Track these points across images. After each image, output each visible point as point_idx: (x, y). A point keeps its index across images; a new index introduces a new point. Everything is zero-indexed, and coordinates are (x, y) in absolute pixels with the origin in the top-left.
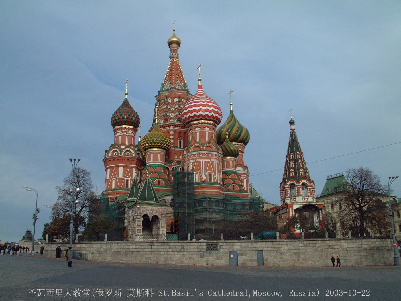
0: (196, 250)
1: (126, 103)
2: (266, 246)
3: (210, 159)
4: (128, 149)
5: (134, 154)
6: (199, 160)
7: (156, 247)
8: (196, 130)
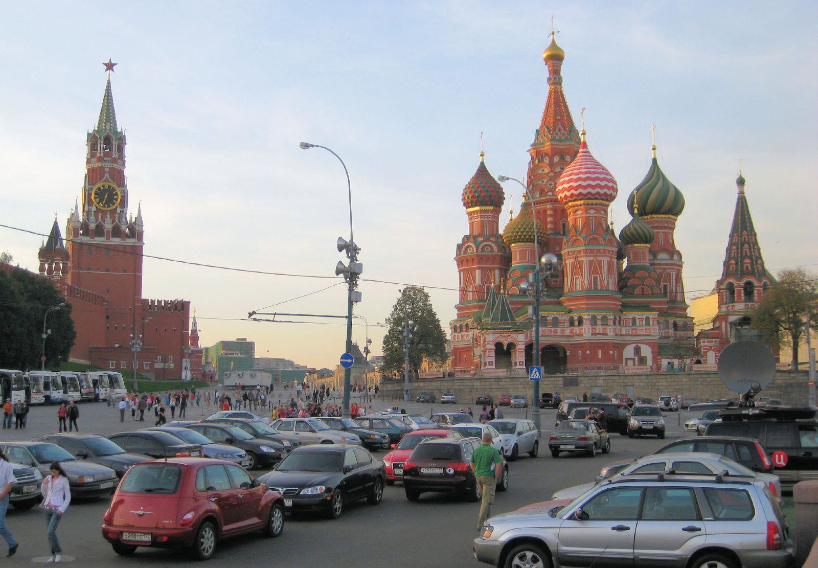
0: (552, 386)
2: (639, 381)
3: (595, 256)
4: (488, 243)
5: (495, 250)
8: (578, 215)
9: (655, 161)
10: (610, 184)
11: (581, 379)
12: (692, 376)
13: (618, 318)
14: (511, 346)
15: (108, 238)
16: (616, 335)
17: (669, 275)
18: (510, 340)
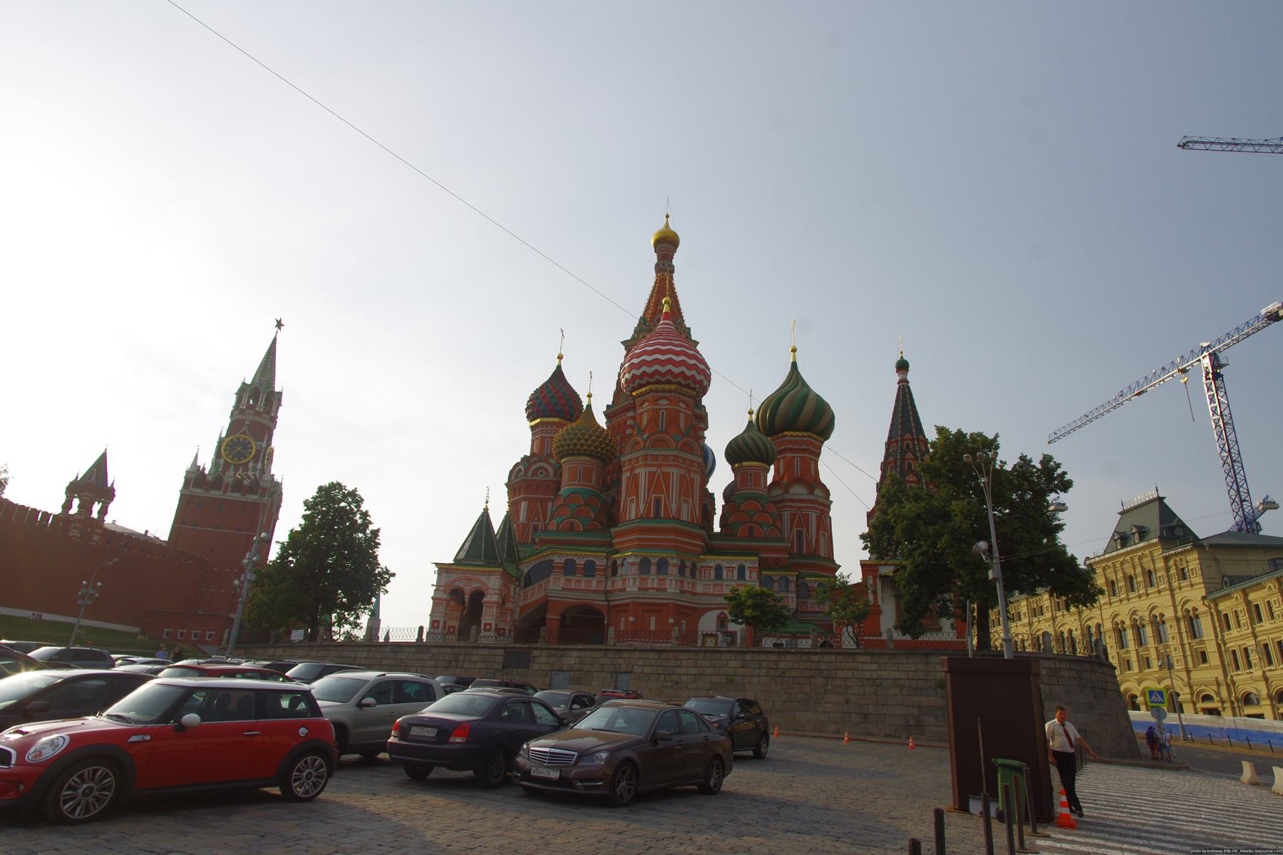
0: (482, 665)
1: (558, 375)
2: (641, 662)
3: (659, 466)
6: (637, 471)
7: (404, 656)
9: (794, 365)
10: (702, 367)
11: (536, 653)
12: (748, 657)
13: (688, 564)
14: (478, 596)
16: (683, 592)
17: (806, 517)
18: (476, 585)
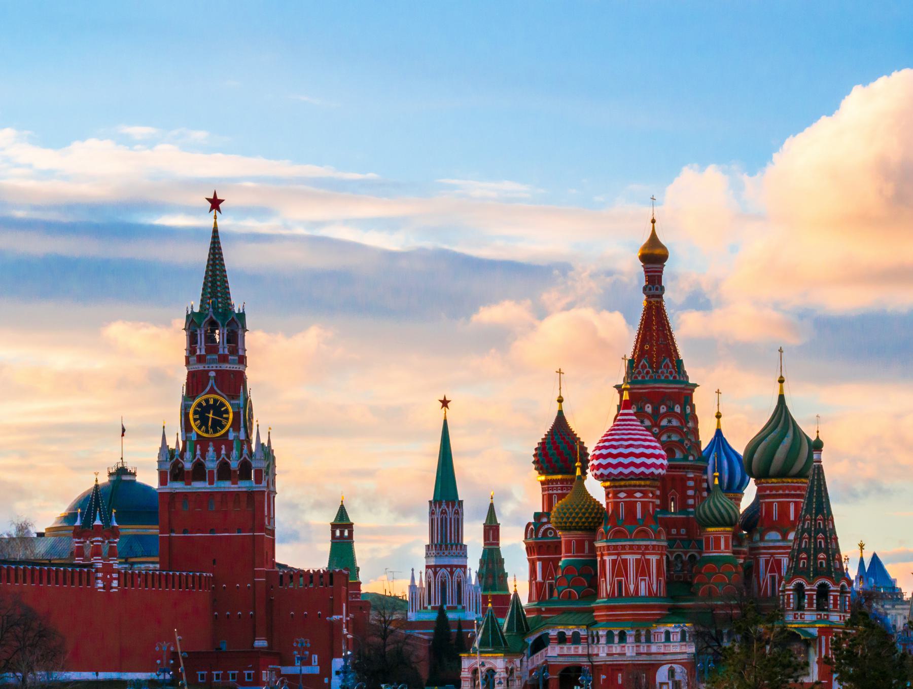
1: (561, 419)
15: (211, 483)
